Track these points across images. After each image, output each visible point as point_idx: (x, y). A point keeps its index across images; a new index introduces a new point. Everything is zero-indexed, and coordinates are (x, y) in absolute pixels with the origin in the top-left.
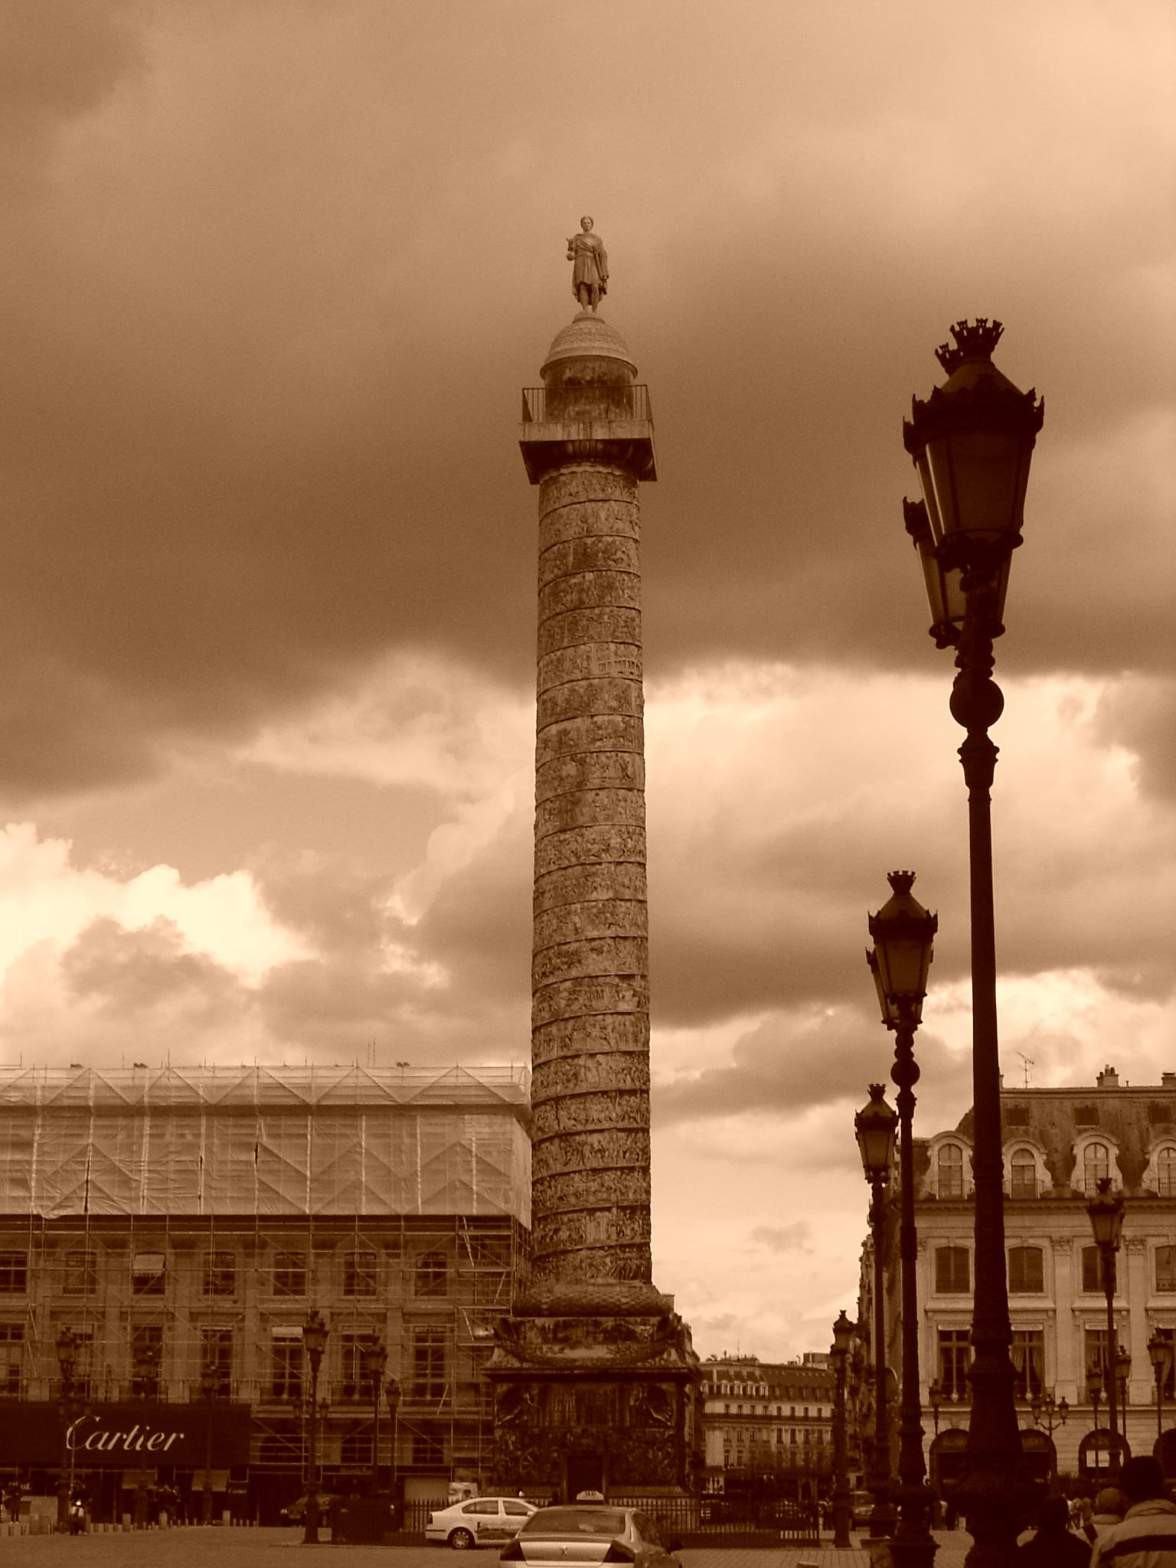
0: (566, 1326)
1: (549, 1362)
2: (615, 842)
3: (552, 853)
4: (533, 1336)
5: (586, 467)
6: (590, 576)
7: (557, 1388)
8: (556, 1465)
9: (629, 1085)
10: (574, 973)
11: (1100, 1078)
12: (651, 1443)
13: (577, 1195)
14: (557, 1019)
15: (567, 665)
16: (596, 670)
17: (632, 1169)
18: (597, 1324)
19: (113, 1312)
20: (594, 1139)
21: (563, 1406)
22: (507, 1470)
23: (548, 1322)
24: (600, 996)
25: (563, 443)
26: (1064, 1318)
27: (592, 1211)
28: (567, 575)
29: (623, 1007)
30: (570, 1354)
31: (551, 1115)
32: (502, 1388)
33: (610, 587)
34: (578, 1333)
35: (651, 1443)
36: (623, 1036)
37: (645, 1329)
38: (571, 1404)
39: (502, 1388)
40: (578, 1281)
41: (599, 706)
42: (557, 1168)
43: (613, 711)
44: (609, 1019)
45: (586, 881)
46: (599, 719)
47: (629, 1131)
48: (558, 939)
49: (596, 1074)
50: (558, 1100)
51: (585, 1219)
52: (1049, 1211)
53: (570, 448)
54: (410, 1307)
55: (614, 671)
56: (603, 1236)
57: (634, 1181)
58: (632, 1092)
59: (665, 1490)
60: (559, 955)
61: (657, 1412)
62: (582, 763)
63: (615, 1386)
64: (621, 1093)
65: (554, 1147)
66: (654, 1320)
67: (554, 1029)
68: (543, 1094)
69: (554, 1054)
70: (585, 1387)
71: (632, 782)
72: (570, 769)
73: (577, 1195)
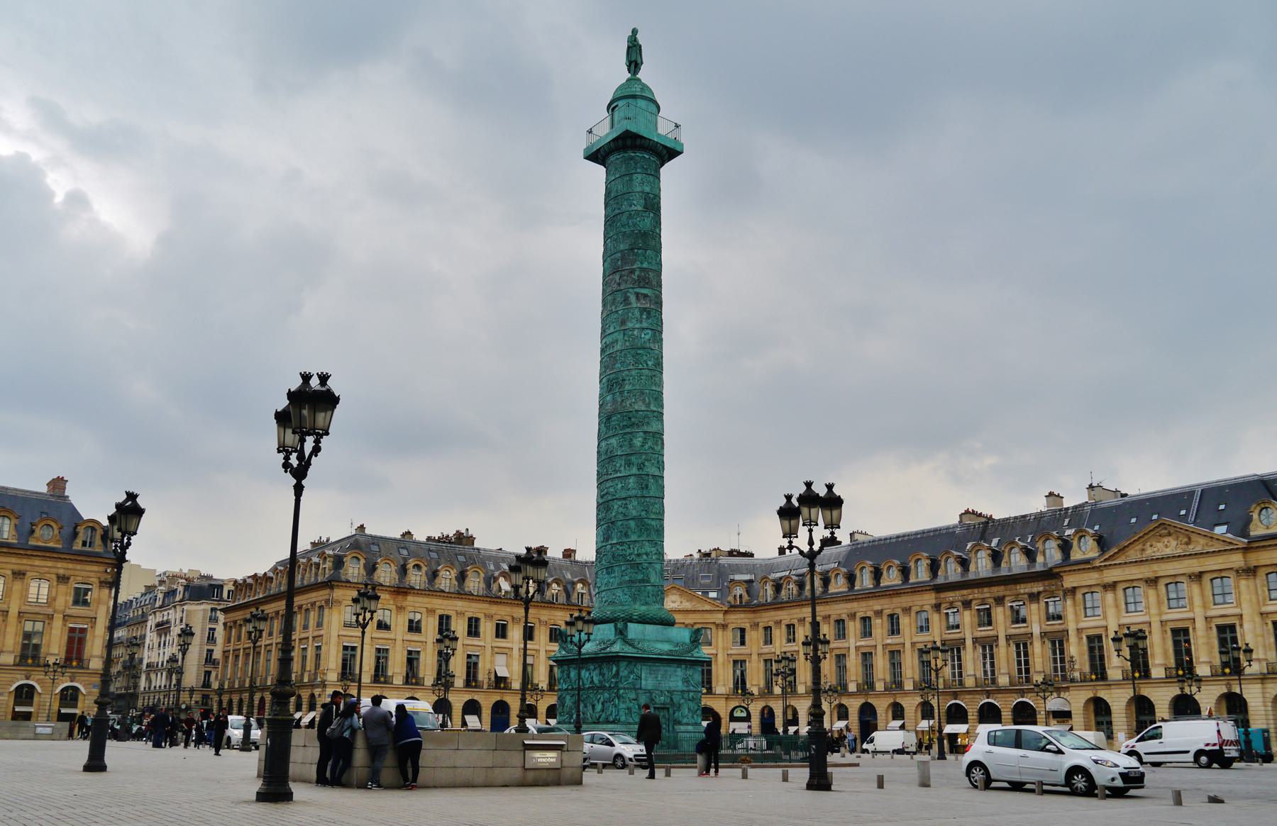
10: (645, 428)
11: (403, 535)
13: (647, 554)
26: (399, 643)
40: (647, 603)
54: (68, 612)
67: (633, 458)
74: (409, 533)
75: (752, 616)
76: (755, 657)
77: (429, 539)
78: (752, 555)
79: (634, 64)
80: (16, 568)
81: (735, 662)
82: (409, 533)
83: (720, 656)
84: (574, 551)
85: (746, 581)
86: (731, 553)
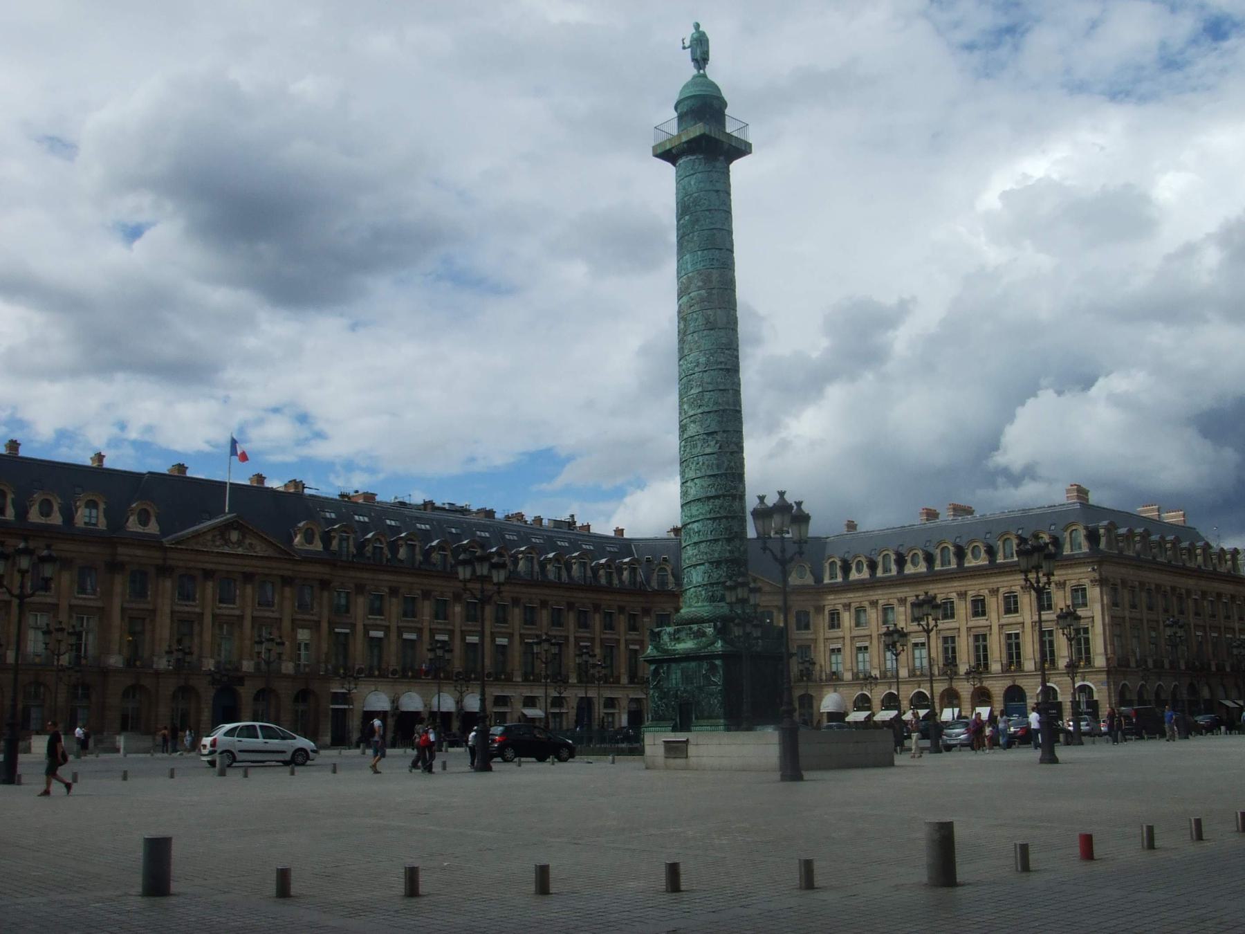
4: (666, 638)
7: (673, 665)
9: (713, 492)
12: (712, 695)
17: (716, 540)
21: (675, 676)
24: (695, 446)
25: (670, 150)
29: (708, 450)
34: (683, 635)
35: (712, 695)
38: (679, 674)
40: (690, 606)
43: (700, 288)
47: (714, 519)
56: (700, 579)
61: (714, 676)
64: (709, 498)
70: (684, 664)
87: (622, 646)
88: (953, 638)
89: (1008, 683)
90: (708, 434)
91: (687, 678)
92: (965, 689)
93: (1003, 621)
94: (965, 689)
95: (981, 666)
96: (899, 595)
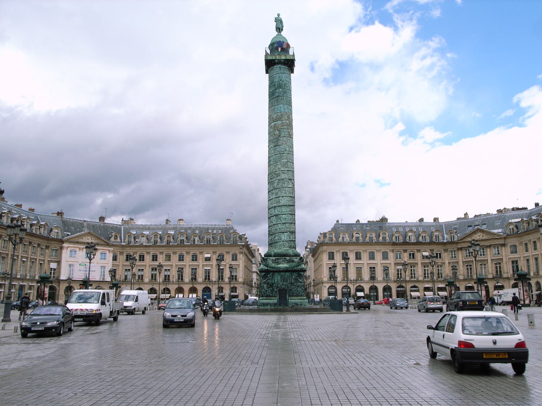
0: (278, 259)
1: (274, 268)
2: (287, 149)
3: (273, 151)
5: (280, 66)
6: (281, 90)
7: (276, 274)
8: (276, 292)
10: (278, 178)
14: (275, 189)
15: (276, 109)
16: (282, 110)
18: (285, 259)
19: (174, 265)
20: (284, 216)
21: (277, 278)
22: (264, 293)
23: (274, 258)
24: (284, 184)
25: (274, 60)
27: (283, 233)
28: (276, 89)
29: (290, 186)
30: (279, 266)
31: (273, 211)
32: (263, 274)
33: (286, 92)
34: (281, 261)
36: (290, 192)
37: (296, 260)
38: (279, 277)
39: (263, 274)
40: (280, 249)
41: (283, 118)
42: (275, 223)
43: (287, 120)
44: (287, 189)
45: (281, 158)
46: (283, 121)
47: (291, 214)
48: (274, 170)
49: (283, 201)
50: (275, 207)
51: (282, 234)
52: (349, 245)
53: (276, 61)
55: (287, 111)
57: (292, 226)
58: (292, 206)
59: (302, 298)
60: (275, 174)
62: (280, 131)
63: (290, 273)
64: (290, 205)
65: (274, 218)
66: (298, 258)
67: (274, 191)
68: (271, 206)
69: (274, 197)
70: (282, 273)
71: (291, 136)
72: (277, 132)
73: (280, 229)
74: (358, 220)
75: (519, 239)
76: (522, 259)
77: (369, 221)
78: (526, 208)
79: (279, 29)
80: (213, 250)
81: (513, 262)
82: (358, 220)
83: (504, 259)
84: (438, 219)
85: (515, 223)
86: (513, 209)
87: (37, 262)
88: (196, 269)
89: (191, 286)
90: (290, 179)
91: (284, 280)
92: (186, 288)
93: (204, 264)
94: (186, 288)
95: (194, 278)
96: (160, 251)
